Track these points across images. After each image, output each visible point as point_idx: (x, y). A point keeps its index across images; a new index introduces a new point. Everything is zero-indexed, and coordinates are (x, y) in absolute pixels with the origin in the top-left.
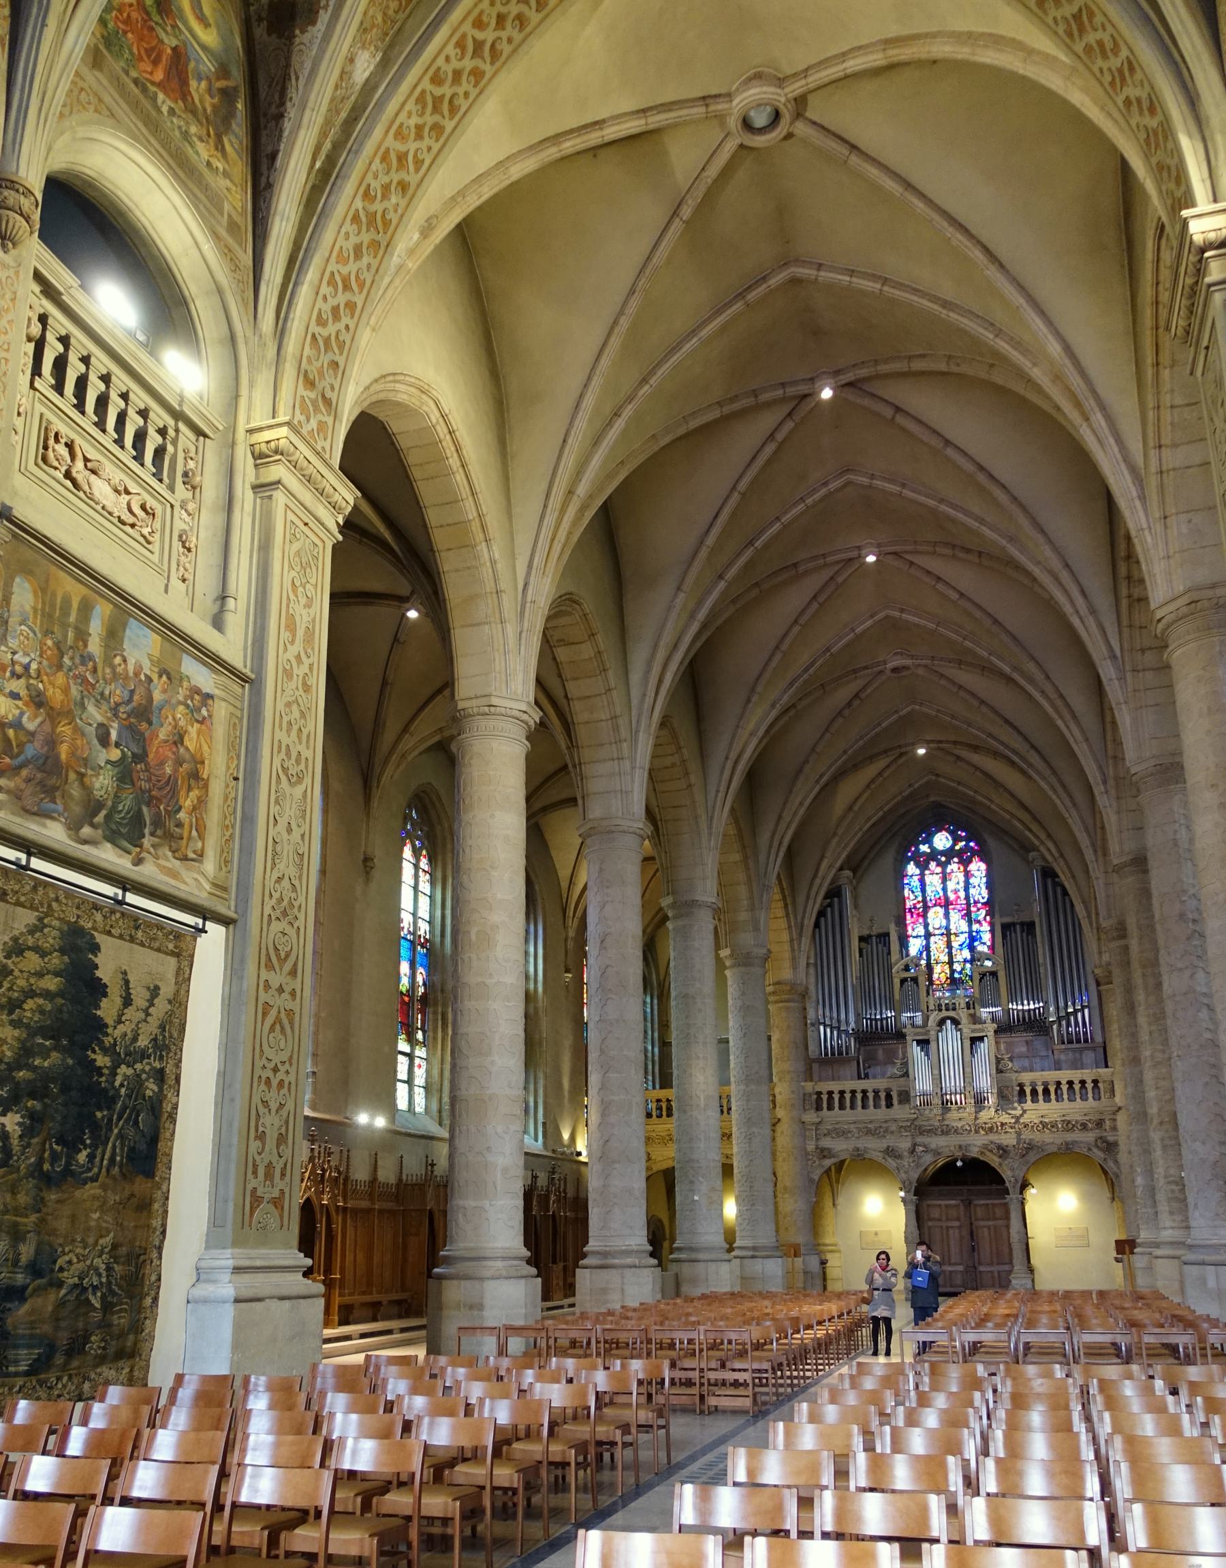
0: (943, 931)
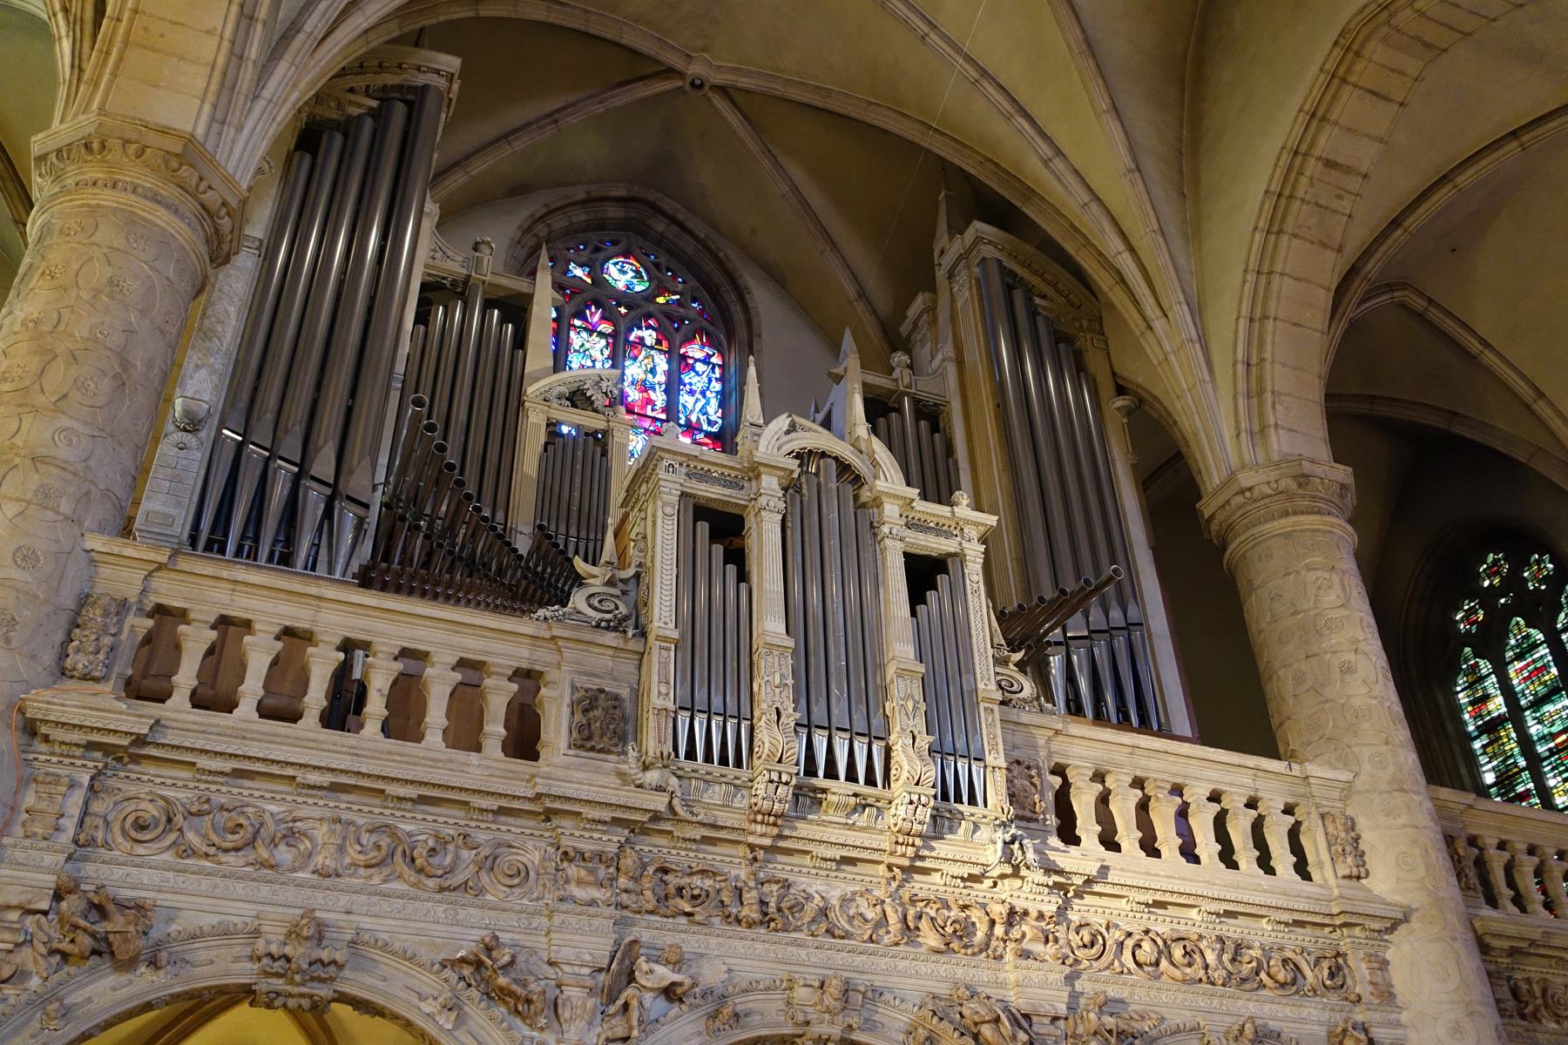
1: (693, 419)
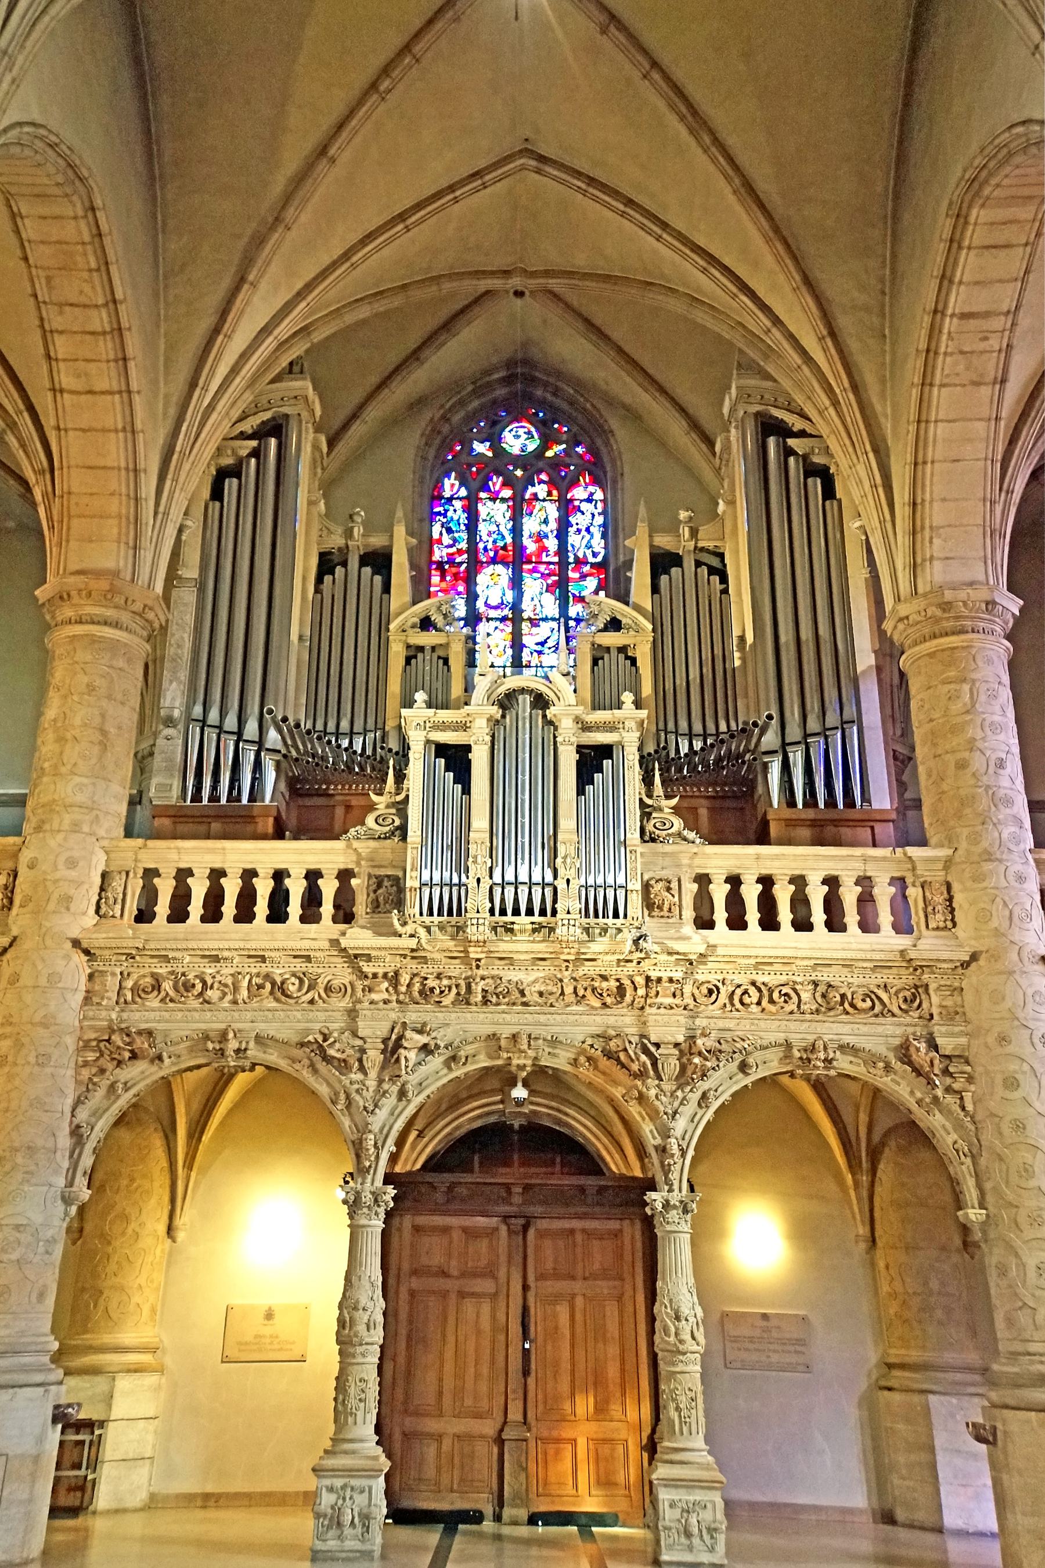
0: (507, 612)
1: (580, 555)
